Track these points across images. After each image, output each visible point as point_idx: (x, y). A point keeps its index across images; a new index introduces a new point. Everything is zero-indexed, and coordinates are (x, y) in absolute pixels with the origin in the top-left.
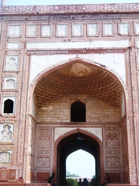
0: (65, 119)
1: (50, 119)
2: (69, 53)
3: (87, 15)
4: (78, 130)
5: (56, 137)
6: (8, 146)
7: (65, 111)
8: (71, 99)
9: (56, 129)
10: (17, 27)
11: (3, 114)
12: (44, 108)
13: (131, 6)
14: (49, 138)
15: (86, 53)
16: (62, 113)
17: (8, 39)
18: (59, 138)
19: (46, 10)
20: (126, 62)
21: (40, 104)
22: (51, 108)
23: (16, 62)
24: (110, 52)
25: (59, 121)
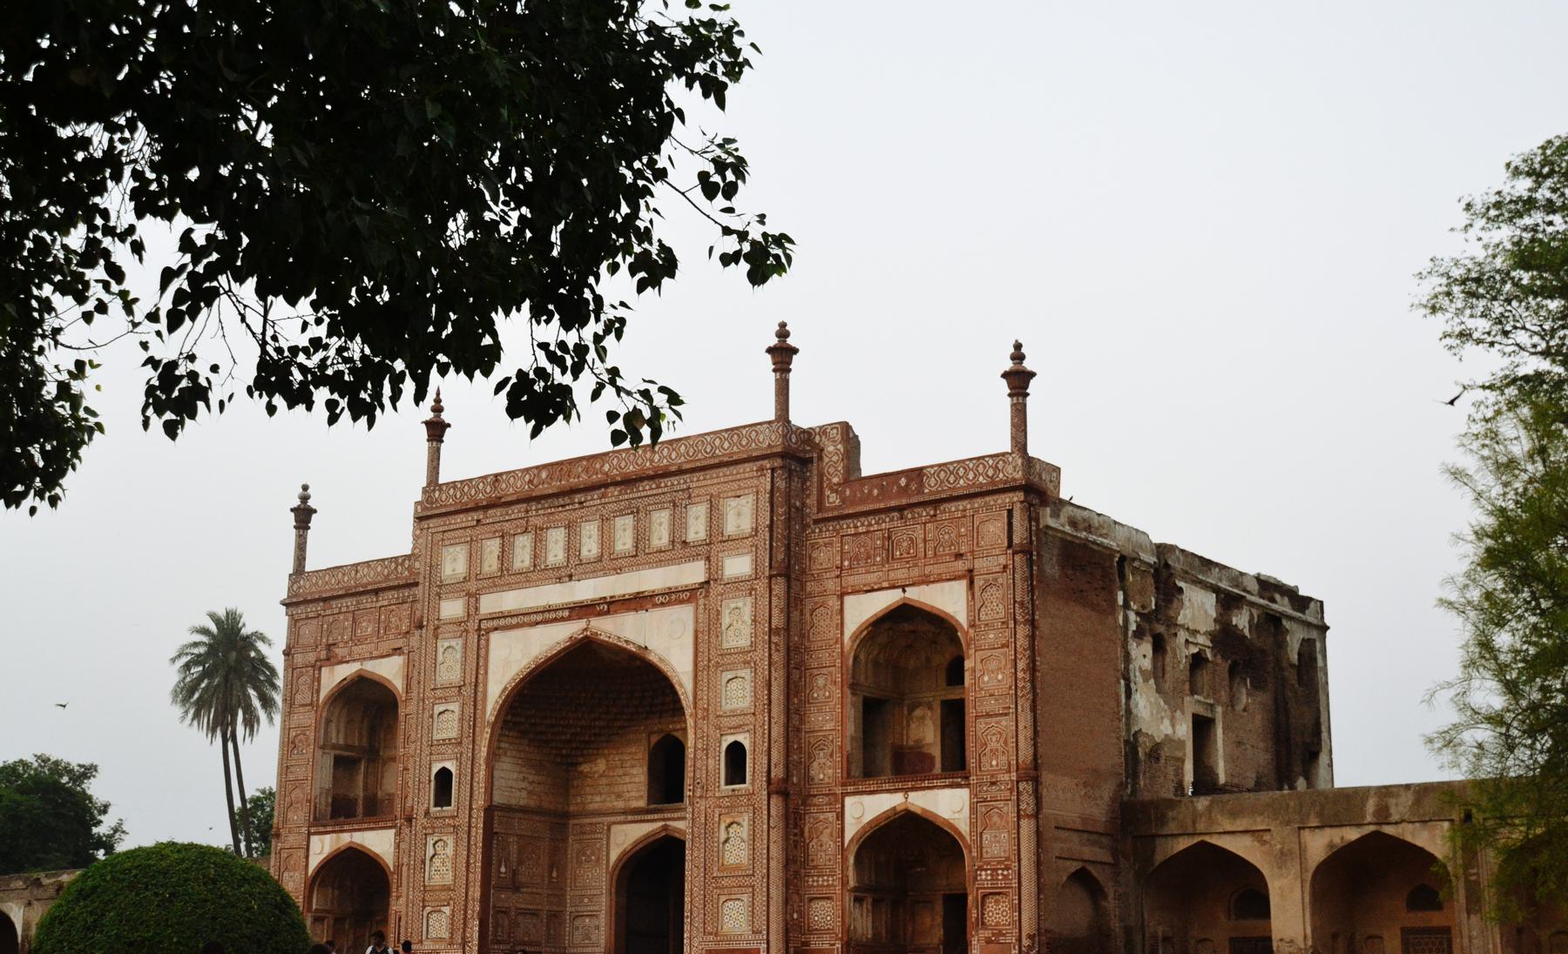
0: (637, 799)
1: (598, 799)
2: (569, 618)
3: (611, 489)
4: (665, 828)
5: (614, 856)
6: (444, 895)
7: (634, 771)
8: (649, 735)
9: (614, 829)
10: (458, 548)
11: (433, 809)
12: (585, 768)
13: (717, 442)
14: (598, 860)
15: (608, 612)
16: (627, 779)
17: (441, 591)
18: (619, 859)
19: (522, 486)
20: (696, 631)
21: (568, 756)
22: (601, 765)
23: (459, 656)
24: (662, 604)
25: (620, 805)
